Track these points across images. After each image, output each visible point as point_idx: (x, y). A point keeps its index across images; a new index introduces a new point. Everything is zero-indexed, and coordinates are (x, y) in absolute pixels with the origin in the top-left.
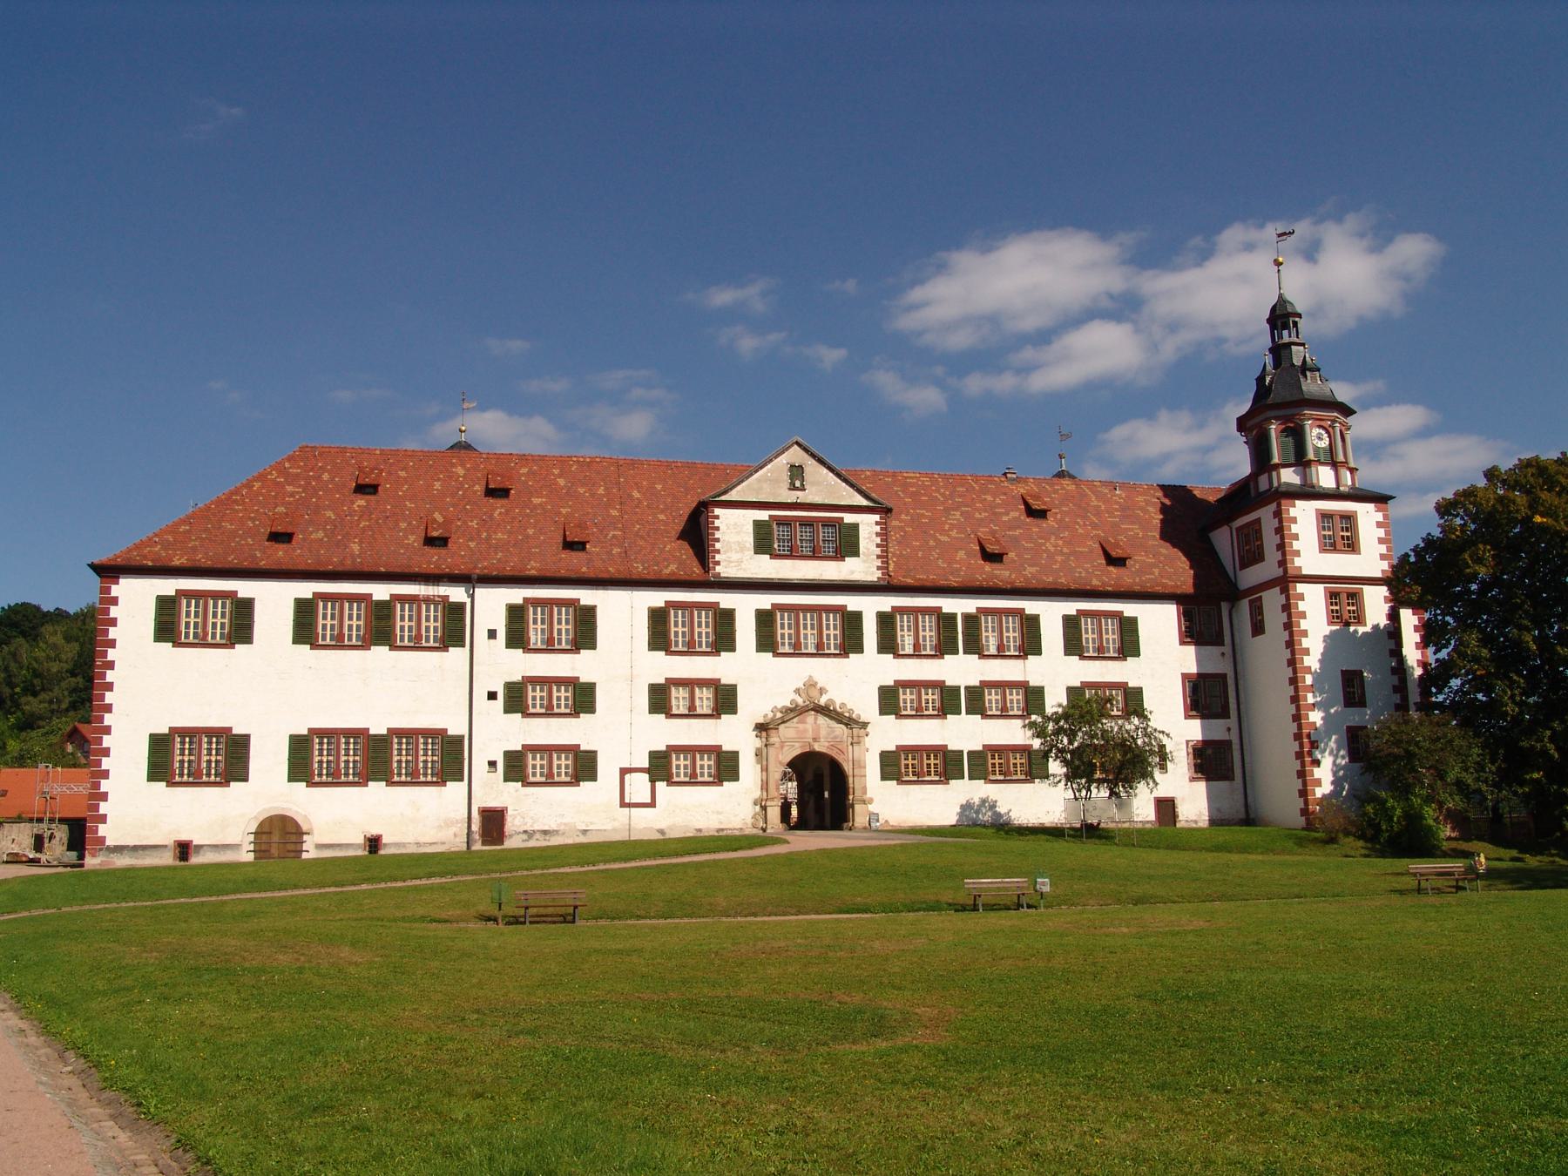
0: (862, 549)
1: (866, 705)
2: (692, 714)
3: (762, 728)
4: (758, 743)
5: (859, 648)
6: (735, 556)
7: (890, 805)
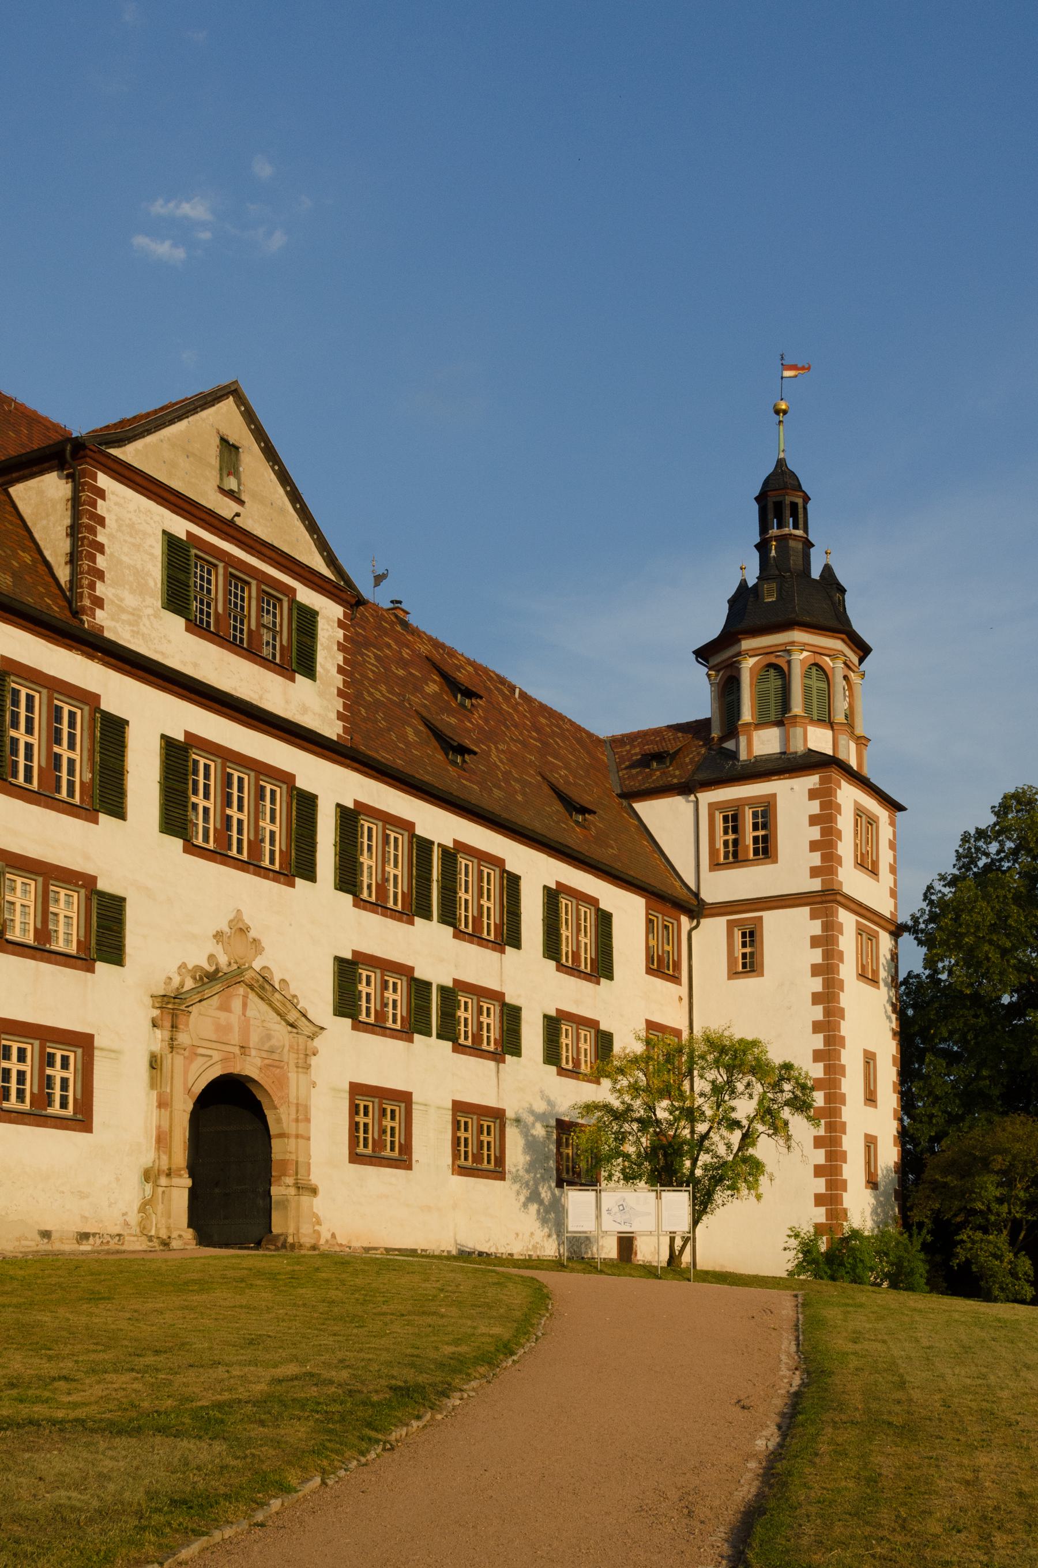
0: (319, 668)
1: (317, 994)
2: (40, 949)
3: (172, 1008)
4: (157, 1040)
5: (309, 873)
6: (130, 600)
7: (340, 1202)
